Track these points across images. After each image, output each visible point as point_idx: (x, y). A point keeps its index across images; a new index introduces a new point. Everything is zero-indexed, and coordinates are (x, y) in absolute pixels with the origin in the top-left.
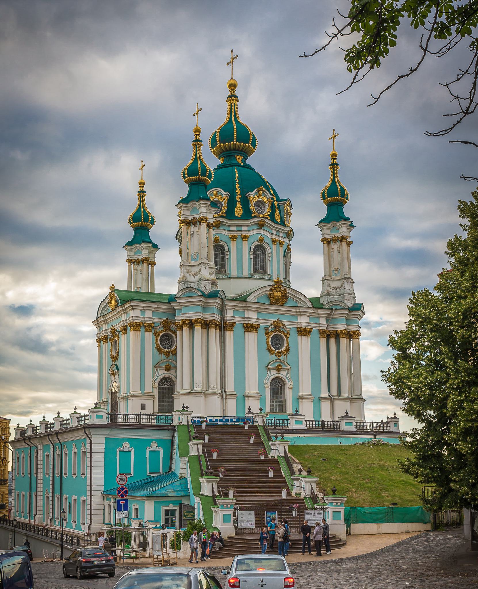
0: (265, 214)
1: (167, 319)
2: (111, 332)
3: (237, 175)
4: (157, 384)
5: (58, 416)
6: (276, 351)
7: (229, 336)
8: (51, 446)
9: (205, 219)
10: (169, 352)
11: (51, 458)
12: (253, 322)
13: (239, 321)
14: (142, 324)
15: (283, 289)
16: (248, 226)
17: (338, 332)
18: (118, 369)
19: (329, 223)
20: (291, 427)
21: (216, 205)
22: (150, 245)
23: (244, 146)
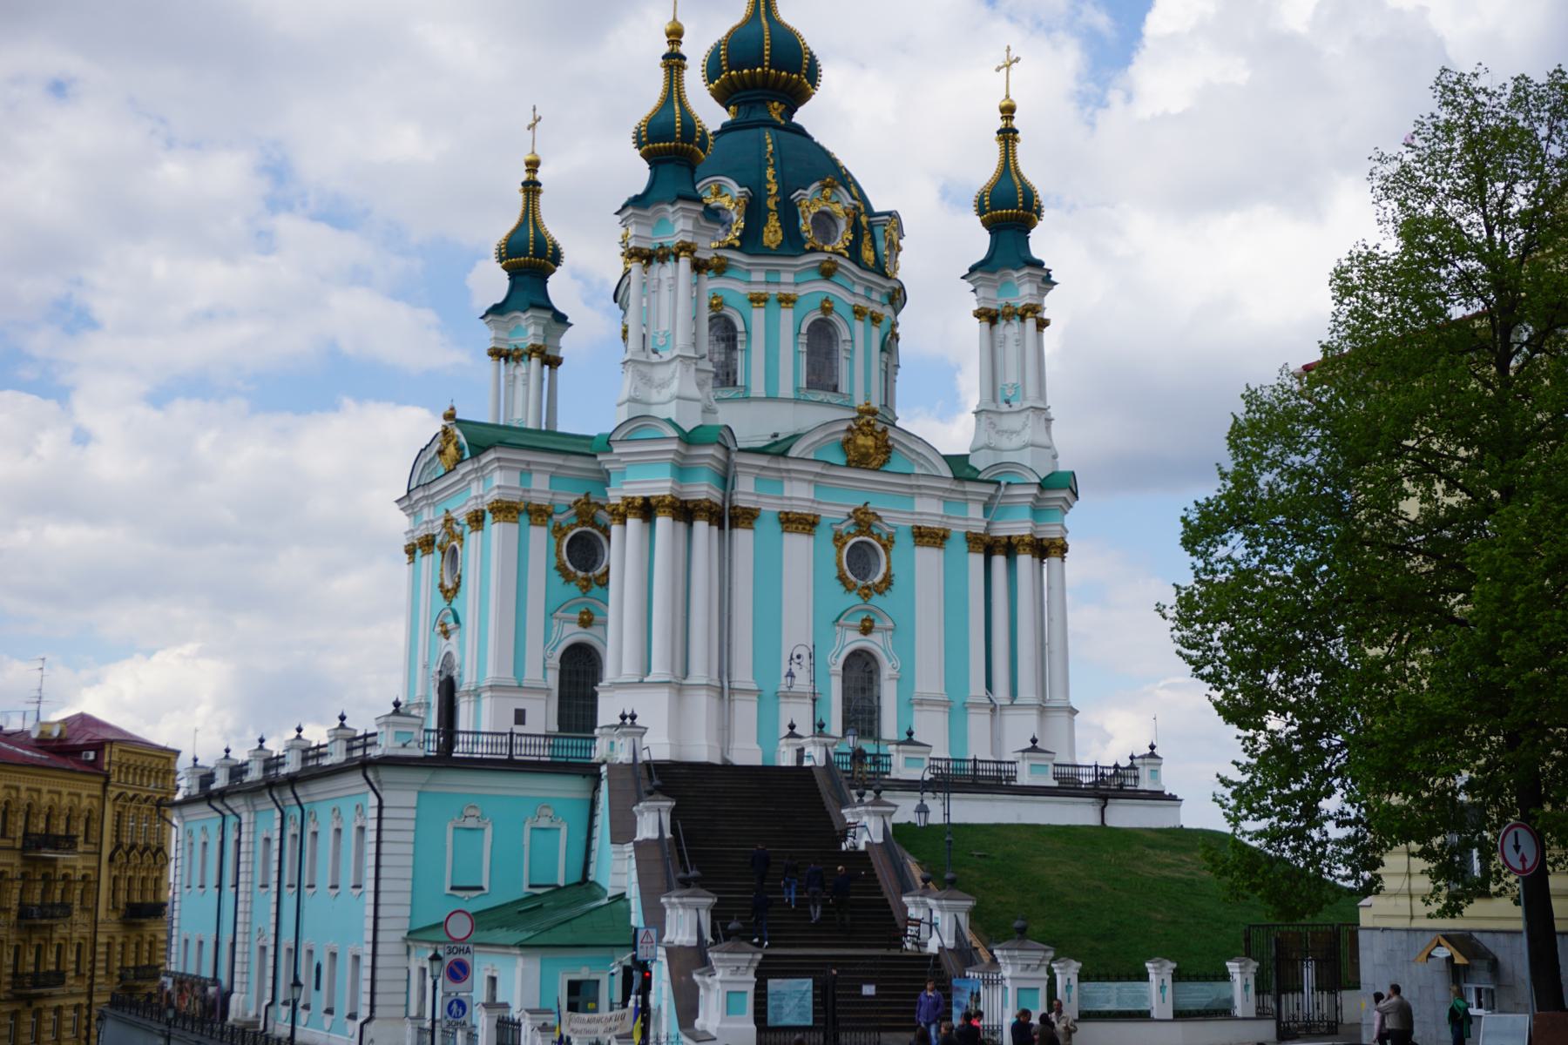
0: (839, 245)
1: (587, 495)
2: (444, 526)
3: (770, 147)
4: (555, 662)
5: (299, 737)
6: (860, 583)
8: (277, 814)
9: (687, 248)
10: (588, 580)
11: (276, 845)
13: (770, 507)
14: (522, 506)
15: (879, 427)
17: (1014, 541)
18: (457, 621)
19: (993, 272)
20: (894, 775)
21: (717, 215)
22: (548, 315)
23: (789, 80)
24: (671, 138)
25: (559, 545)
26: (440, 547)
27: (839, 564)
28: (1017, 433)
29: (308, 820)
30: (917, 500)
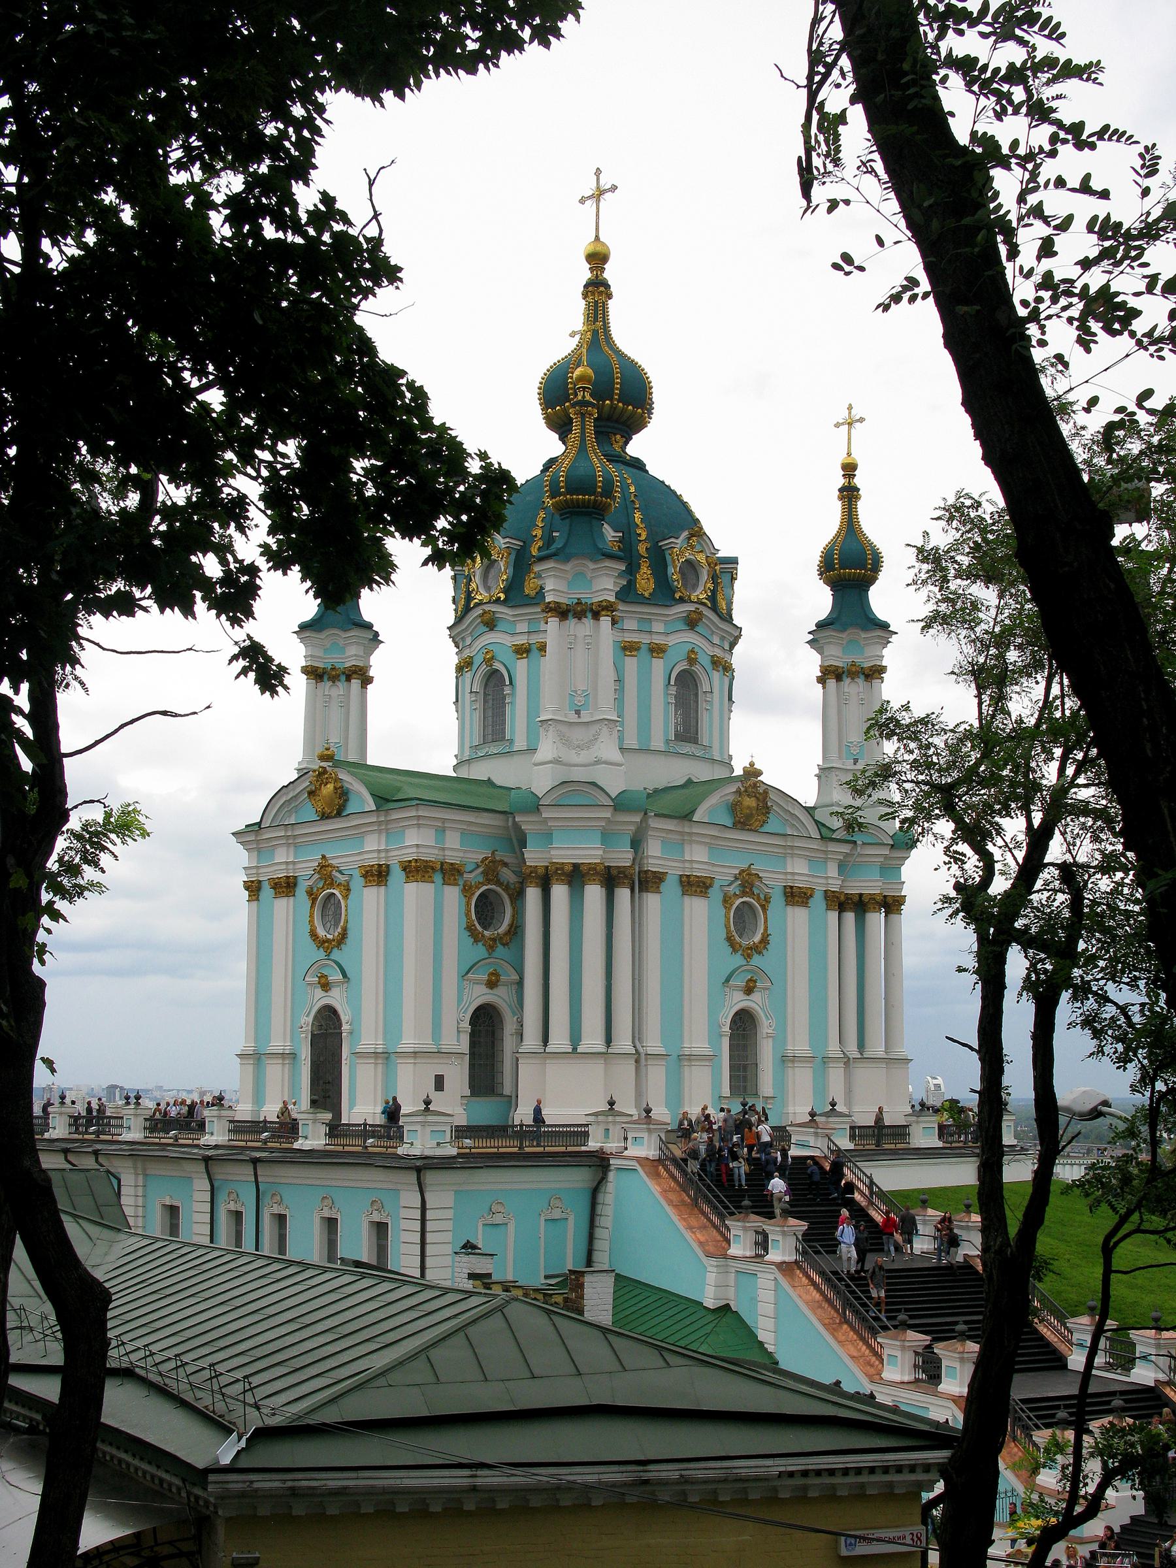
0: (700, 594)
1: (493, 853)
3: (632, 489)
10: (494, 940)
12: (700, 872)
14: (439, 867)
16: (666, 623)
18: (344, 975)
23: (633, 414)
24: (594, 493)
26: (312, 894)
27: (727, 927)
29: (266, 1200)
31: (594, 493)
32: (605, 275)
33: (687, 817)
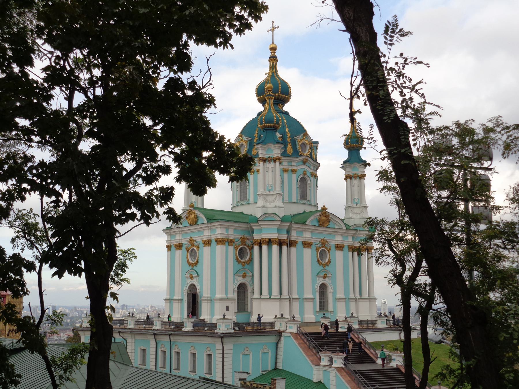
0: (307, 153)
3: (285, 121)
4: (236, 290)
7: (293, 250)
13: (300, 240)
16: (296, 163)
19: (352, 163)
23: (285, 98)
25: (236, 251)
26: (187, 249)
27: (317, 257)
28: (359, 214)
29: (173, 347)
30: (336, 236)
31: (272, 122)
32: (276, 54)
33: (304, 223)
